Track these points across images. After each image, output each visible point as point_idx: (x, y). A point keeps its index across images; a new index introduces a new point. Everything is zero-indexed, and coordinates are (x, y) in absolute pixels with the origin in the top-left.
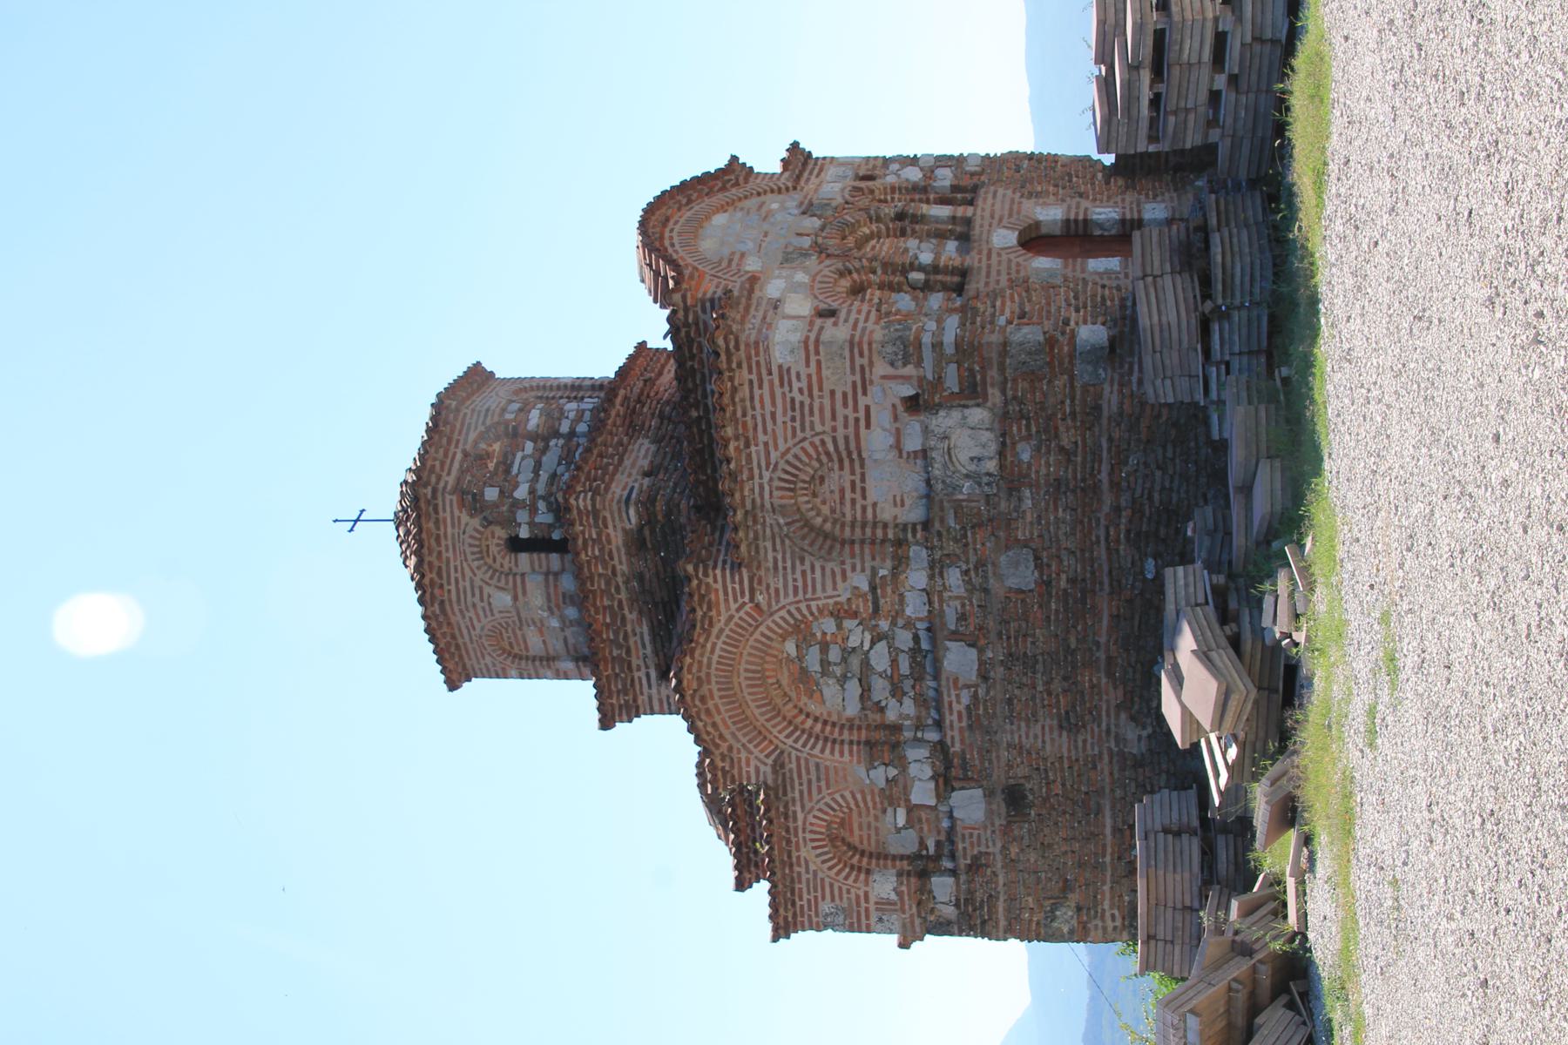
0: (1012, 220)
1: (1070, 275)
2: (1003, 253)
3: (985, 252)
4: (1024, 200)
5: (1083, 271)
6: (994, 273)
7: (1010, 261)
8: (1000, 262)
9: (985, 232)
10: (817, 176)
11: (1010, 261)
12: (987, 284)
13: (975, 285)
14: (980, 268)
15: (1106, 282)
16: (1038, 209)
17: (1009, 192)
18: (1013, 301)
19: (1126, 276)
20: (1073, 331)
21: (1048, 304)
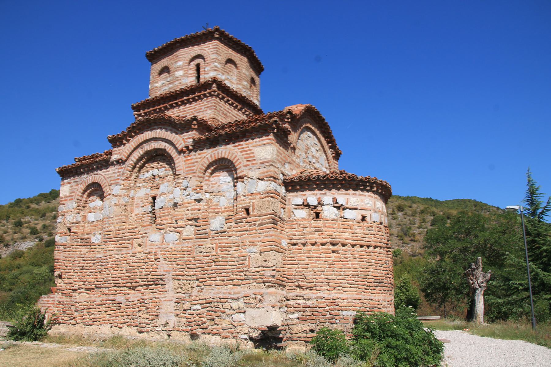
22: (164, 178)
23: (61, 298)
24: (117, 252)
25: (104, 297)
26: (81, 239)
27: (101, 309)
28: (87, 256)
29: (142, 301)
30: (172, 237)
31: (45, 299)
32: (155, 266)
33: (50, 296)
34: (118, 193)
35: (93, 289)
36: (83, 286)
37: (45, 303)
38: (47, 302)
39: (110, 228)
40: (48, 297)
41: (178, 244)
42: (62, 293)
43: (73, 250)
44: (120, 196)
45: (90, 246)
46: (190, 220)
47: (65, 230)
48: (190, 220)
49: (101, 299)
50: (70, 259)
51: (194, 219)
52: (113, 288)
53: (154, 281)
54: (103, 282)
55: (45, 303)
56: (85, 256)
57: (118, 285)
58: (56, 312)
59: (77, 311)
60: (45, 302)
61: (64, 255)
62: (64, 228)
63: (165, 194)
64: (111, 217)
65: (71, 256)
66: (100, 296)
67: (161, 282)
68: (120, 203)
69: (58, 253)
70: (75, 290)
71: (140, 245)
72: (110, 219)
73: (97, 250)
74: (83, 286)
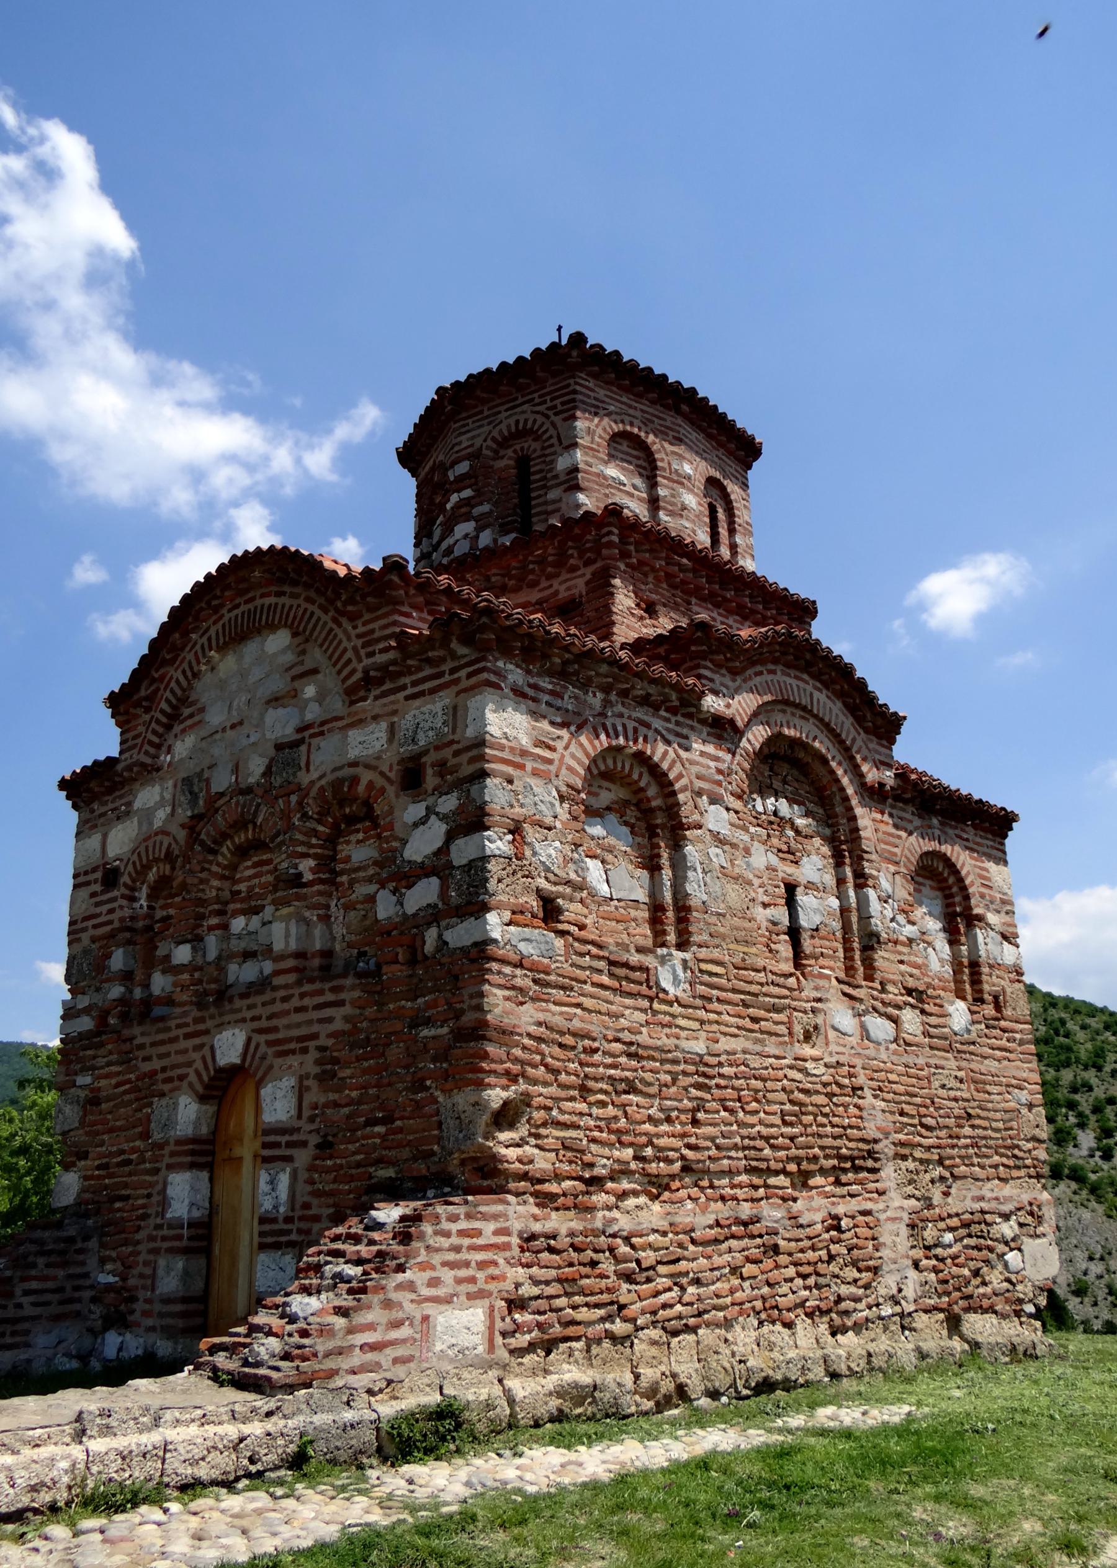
0: (263, 1048)
1: (167, 1151)
2: (206, 1051)
3: (201, 1027)
4: (313, 1055)
5: (170, 1167)
6: (162, 1049)
7: (189, 1064)
8: (186, 1051)
9: (239, 1016)
10: (407, 698)
11: (189, 1064)
12: (141, 1047)
13: (140, 1034)
14: (169, 1029)
15: (155, 1199)
16: (288, 1082)
17: (338, 1025)
18: (118, 1085)
19: (159, 1227)
20: (74, 1164)
21: (111, 1131)
22: (806, 837)
23: (536, 1218)
24: (749, 1045)
25: (720, 1211)
26: (612, 963)
27: (717, 1261)
28: (643, 1038)
29: (834, 1223)
30: (880, 1027)
31: (454, 1227)
32: (852, 1110)
33: (482, 1209)
34: (725, 831)
35: (672, 1177)
36: (633, 1166)
37: (457, 1249)
38: (466, 1242)
39: (716, 954)
40: (469, 1216)
41: (895, 1053)
42: (536, 1194)
43: (588, 1002)
44: (734, 846)
45: (651, 999)
46: (909, 992)
47: (534, 904)
48: (909, 992)
49: (710, 1219)
50: (569, 1040)
51: (916, 990)
52: (744, 1178)
53: (852, 1159)
54: (713, 1152)
55: (457, 1249)
56: (639, 1038)
57: (763, 1165)
58: (527, 1290)
59: (629, 1278)
60: (455, 1240)
61: (541, 1016)
62: (527, 889)
63: (817, 889)
64: (720, 914)
65: (576, 1024)
66: (704, 1210)
67: (870, 1163)
68: (737, 870)
69: (507, 999)
70: (595, 1182)
71: (807, 1037)
72: (714, 919)
73: (682, 1022)
74: (633, 1166)
